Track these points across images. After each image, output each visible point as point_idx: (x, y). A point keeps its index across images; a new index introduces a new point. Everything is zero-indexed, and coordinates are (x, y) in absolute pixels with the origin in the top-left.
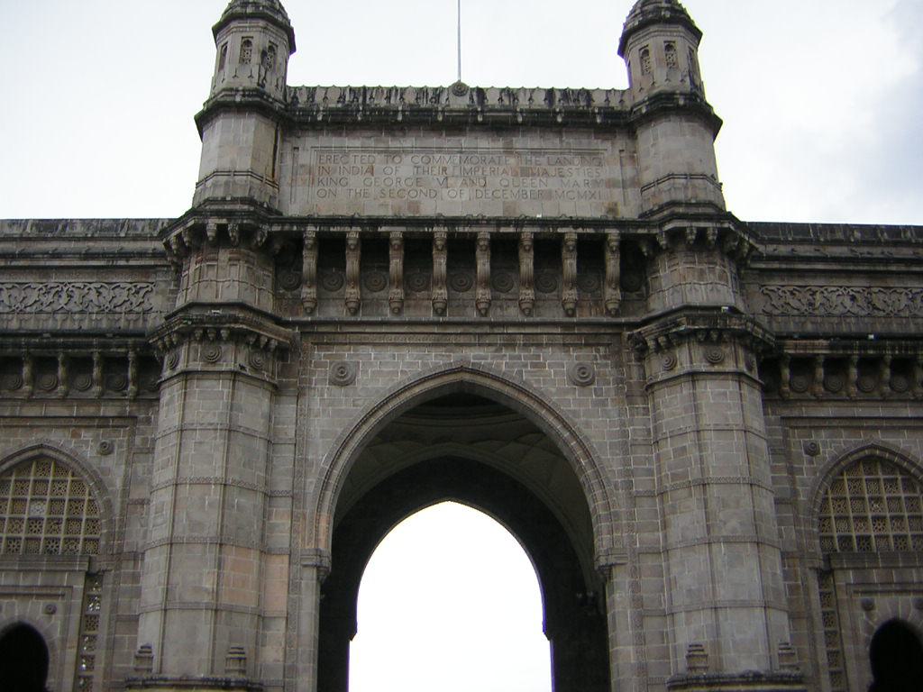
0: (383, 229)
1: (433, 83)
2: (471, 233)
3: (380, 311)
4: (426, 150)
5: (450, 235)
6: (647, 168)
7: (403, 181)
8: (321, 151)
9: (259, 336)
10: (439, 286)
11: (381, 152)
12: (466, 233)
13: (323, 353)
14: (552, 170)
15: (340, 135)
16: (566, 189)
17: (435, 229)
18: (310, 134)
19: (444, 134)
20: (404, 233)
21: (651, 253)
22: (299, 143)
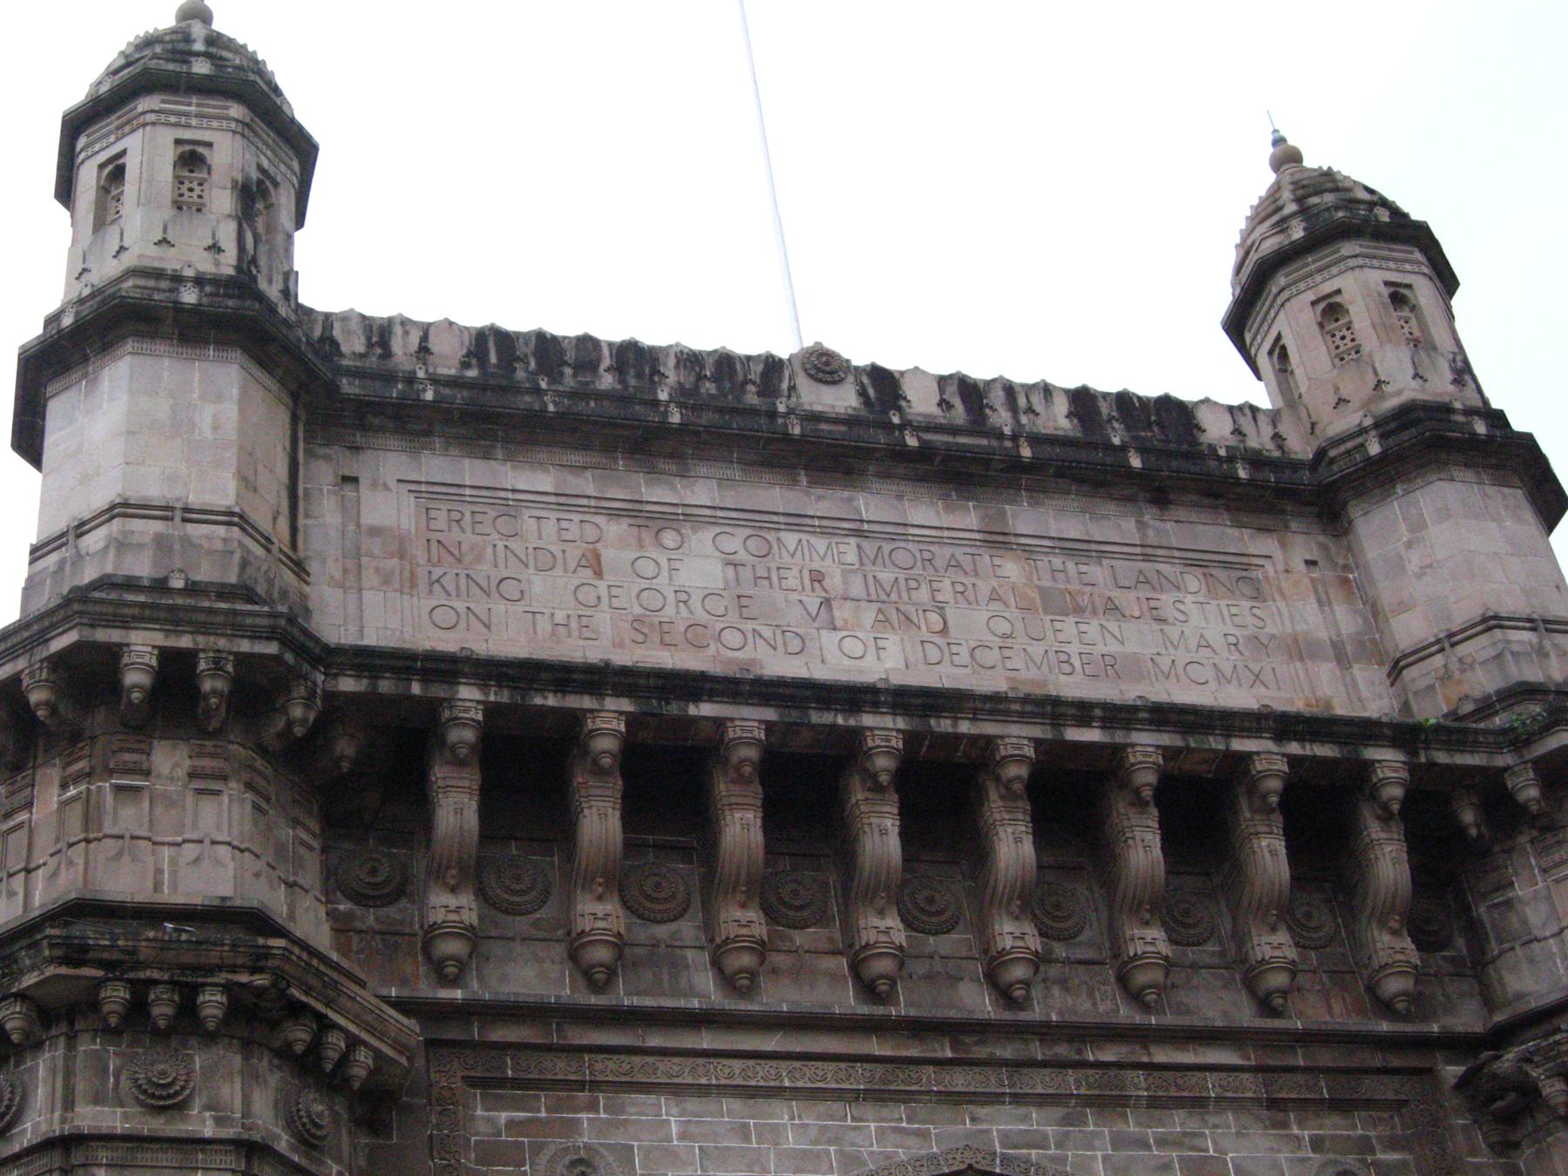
0: (706, 709)
1: (746, 344)
2: (974, 739)
3: (683, 983)
4: (758, 521)
5: (911, 738)
6: (1404, 606)
7: (695, 602)
8: (430, 493)
9: (325, 1025)
10: (880, 903)
11: (615, 514)
12: (958, 737)
13: (504, 1116)
14: (1128, 601)
15: (487, 456)
16: (1182, 657)
17: (868, 720)
18: (393, 442)
19: (804, 480)
20: (769, 727)
21: (1484, 830)
22: (362, 465)
